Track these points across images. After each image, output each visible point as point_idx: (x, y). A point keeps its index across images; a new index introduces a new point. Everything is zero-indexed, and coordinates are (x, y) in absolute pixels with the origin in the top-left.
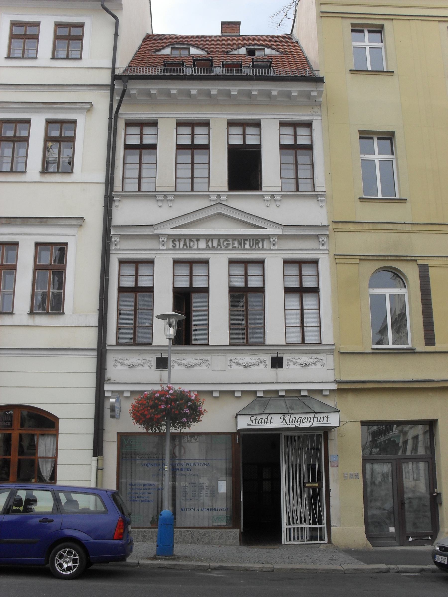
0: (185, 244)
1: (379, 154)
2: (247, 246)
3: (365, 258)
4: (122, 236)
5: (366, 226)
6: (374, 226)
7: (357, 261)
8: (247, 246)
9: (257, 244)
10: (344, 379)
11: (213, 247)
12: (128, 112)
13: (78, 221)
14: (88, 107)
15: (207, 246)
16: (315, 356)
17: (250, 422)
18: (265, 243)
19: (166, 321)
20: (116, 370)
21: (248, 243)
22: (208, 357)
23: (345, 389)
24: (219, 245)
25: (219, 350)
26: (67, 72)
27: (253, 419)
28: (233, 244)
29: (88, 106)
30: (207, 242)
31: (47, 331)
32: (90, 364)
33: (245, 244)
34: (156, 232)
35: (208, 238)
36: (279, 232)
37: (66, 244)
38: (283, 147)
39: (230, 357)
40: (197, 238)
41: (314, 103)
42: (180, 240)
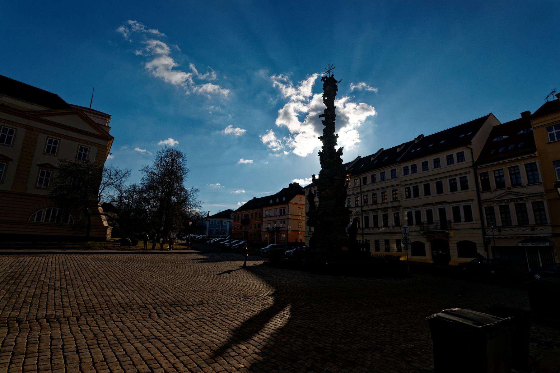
12: (479, 172)
13: (472, 200)
14: (469, 172)
25: (515, 227)
26: (462, 165)
31: (469, 225)
32: (480, 231)
35: (507, 200)
40: (504, 200)
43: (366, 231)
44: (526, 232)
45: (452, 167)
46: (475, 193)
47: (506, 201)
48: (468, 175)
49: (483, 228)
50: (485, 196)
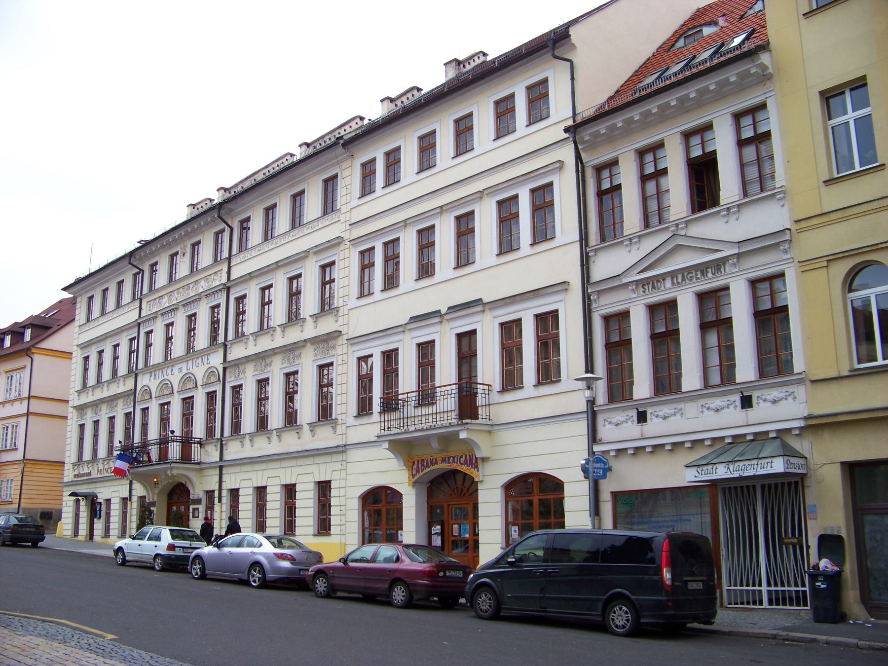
0: (653, 287)
1: (846, 113)
2: (710, 275)
3: (833, 259)
4: (599, 292)
5: (833, 216)
6: (844, 212)
7: (825, 264)
8: (710, 275)
9: (719, 269)
10: (816, 412)
11: (678, 283)
12: (591, 159)
13: (563, 286)
15: (673, 283)
16: (784, 389)
17: (697, 474)
18: (727, 267)
19: (584, 383)
20: (605, 431)
21: (709, 270)
22: (681, 406)
23: (816, 425)
24: (683, 279)
25: (693, 396)
27: (699, 470)
28: (696, 275)
29: (558, 165)
30: (672, 278)
32: (582, 427)
33: (707, 272)
34: (625, 281)
35: (673, 274)
36: (736, 251)
37: (557, 311)
38: (741, 143)
39: (702, 402)
40: (663, 277)
41: (765, 77)
42: (648, 284)
43: (234, 451)
44: (725, 418)
45: (512, 147)
46: (575, 251)
47: (668, 283)
48: (555, 179)
49: (592, 414)
50: (606, 265)
